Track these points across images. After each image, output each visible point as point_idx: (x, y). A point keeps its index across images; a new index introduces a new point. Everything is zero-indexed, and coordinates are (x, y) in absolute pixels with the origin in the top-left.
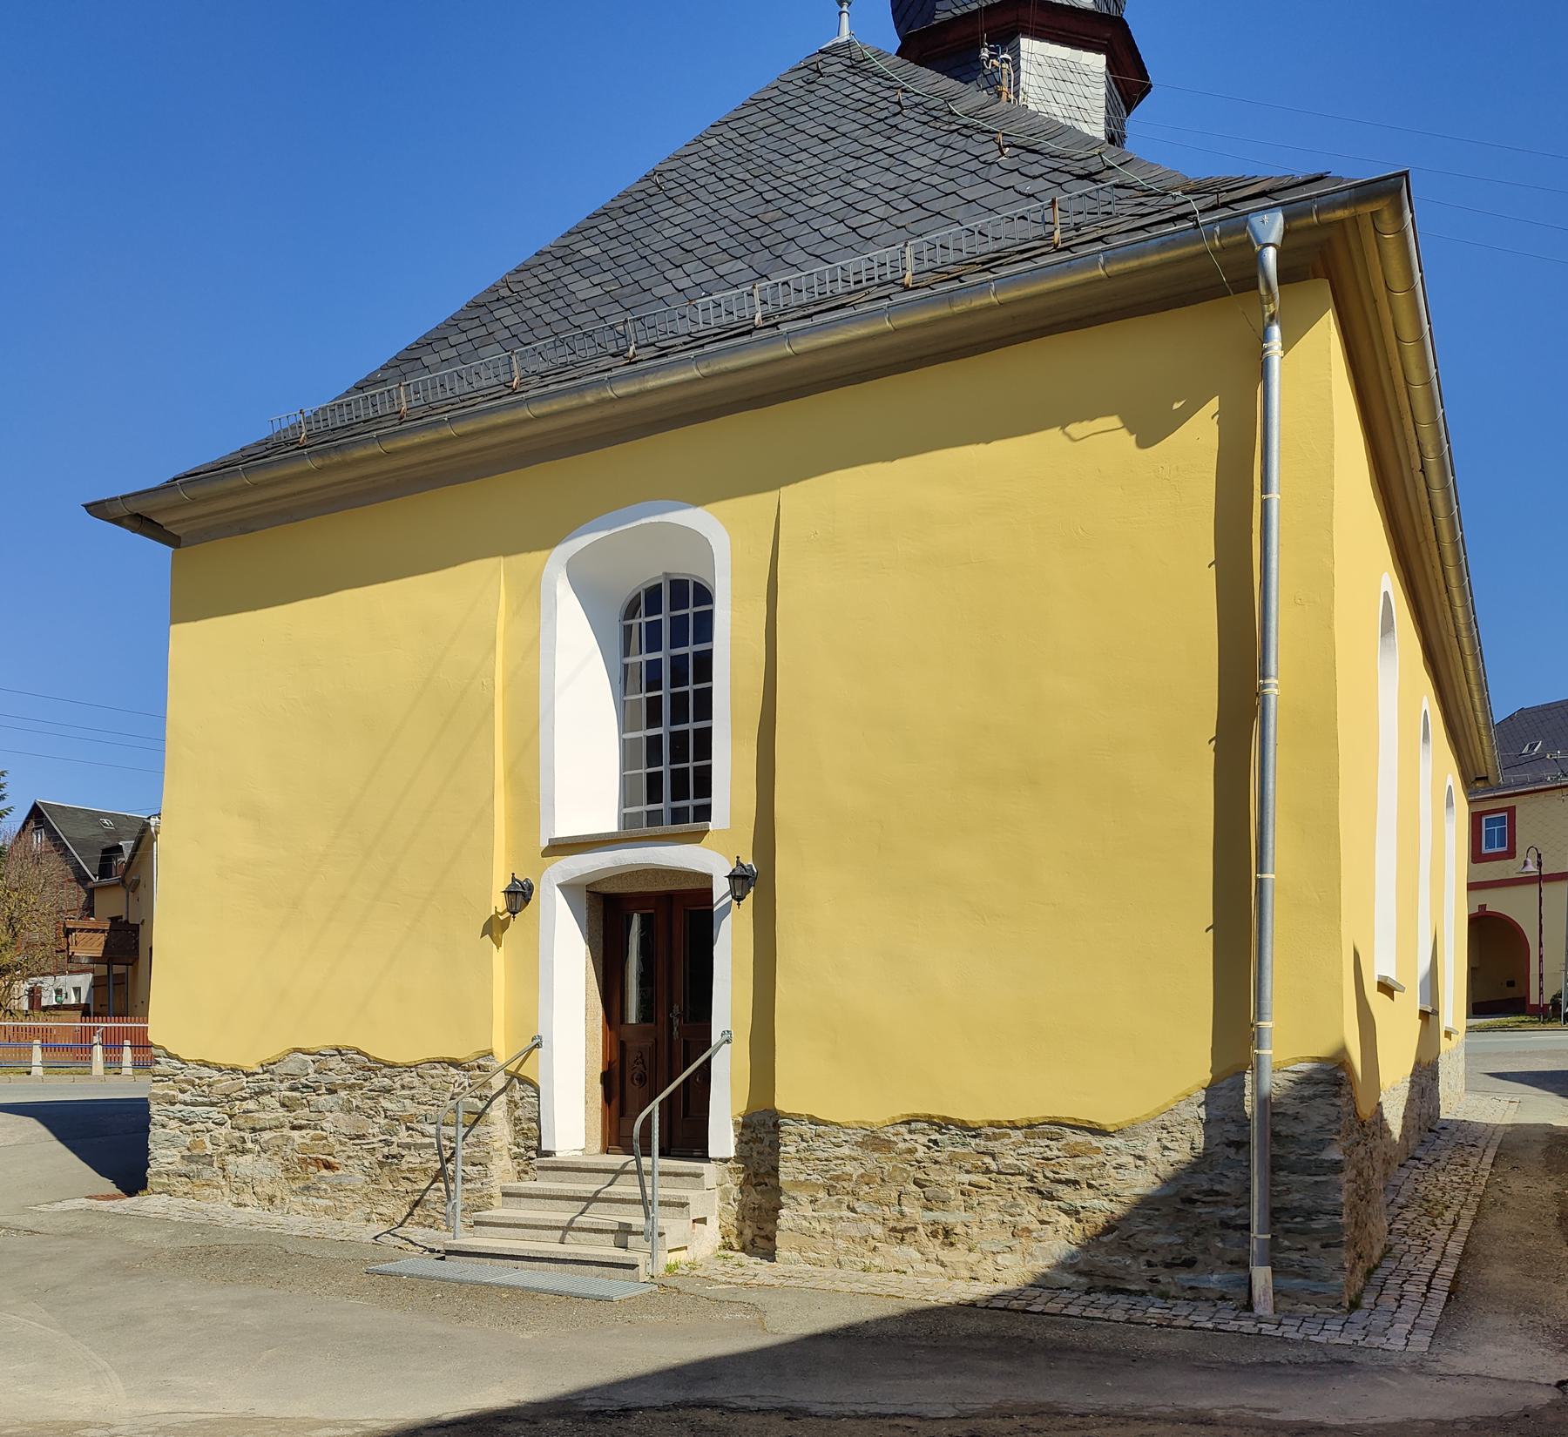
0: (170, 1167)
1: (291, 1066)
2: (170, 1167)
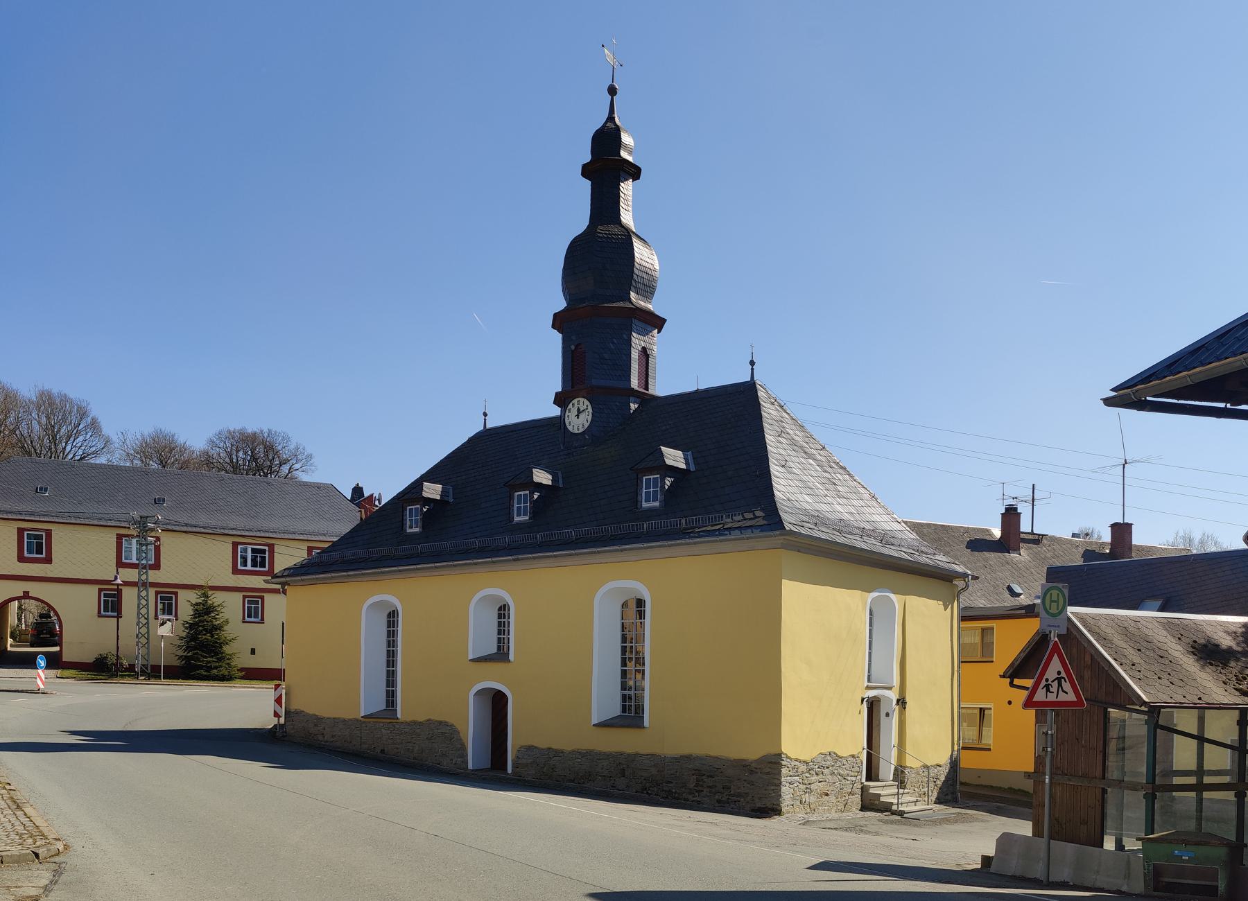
1: (819, 760)
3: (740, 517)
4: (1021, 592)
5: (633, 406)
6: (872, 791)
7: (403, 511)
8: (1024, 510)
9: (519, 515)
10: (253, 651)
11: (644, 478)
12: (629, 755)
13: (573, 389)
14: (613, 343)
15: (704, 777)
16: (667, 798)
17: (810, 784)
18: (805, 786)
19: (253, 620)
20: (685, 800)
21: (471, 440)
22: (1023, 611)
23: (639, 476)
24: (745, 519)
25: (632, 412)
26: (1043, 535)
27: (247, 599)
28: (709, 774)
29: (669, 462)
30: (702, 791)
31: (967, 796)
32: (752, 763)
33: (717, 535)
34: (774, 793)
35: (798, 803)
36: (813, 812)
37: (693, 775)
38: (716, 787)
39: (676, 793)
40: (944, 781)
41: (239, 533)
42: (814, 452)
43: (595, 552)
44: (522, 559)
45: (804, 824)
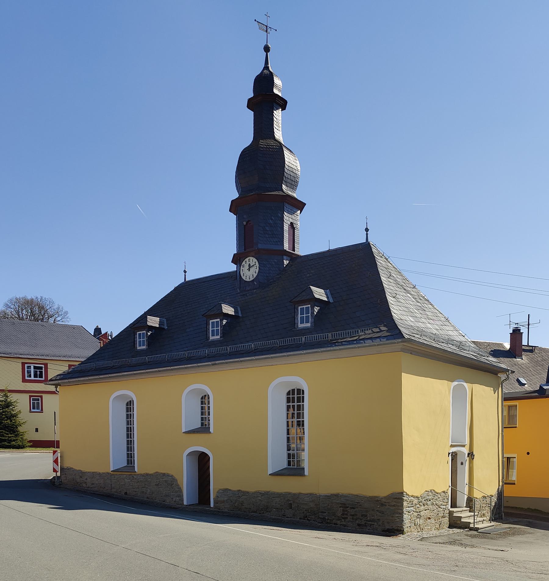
0: (408, 525)
2: (408, 525)
3: (370, 331)
4: (526, 383)
5: (286, 262)
6: (455, 515)
7: (134, 336)
8: (524, 330)
9: (213, 335)
10: (37, 430)
11: (300, 307)
12: (294, 494)
13: (245, 251)
14: (272, 219)
15: (348, 508)
16: (322, 523)
17: (420, 512)
18: (417, 514)
19: (36, 410)
20: (335, 524)
21: (176, 289)
22: (537, 394)
23: (296, 306)
24: (374, 332)
25: (285, 266)
26: (535, 347)
27: (32, 398)
28: (351, 506)
29: (317, 296)
30: (347, 518)
31: (508, 514)
32: (382, 499)
33: (355, 344)
34: (399, 519)
35: (413, 525)
36: (422, 530)
37: (340, 507)
38: (356, 515)
39: (328, 519)
40: (494, 506)
41: (25, 357)
42: (409, 289)
43: (269, 358)
44: (219, 364)
45: (421, 540)
